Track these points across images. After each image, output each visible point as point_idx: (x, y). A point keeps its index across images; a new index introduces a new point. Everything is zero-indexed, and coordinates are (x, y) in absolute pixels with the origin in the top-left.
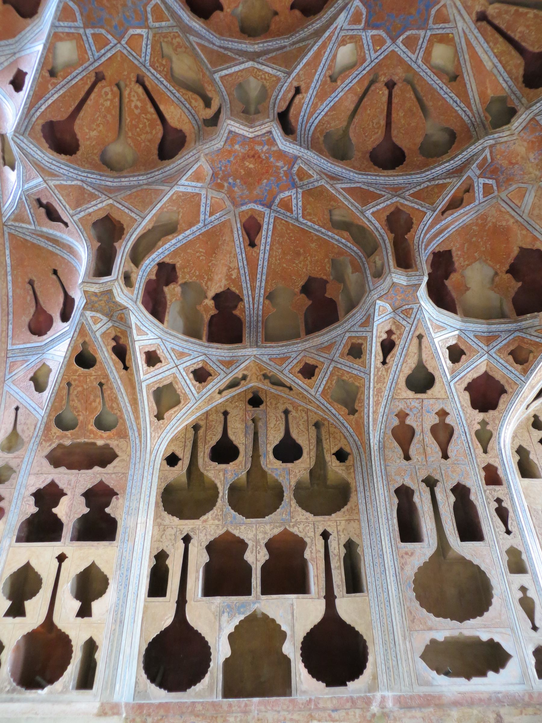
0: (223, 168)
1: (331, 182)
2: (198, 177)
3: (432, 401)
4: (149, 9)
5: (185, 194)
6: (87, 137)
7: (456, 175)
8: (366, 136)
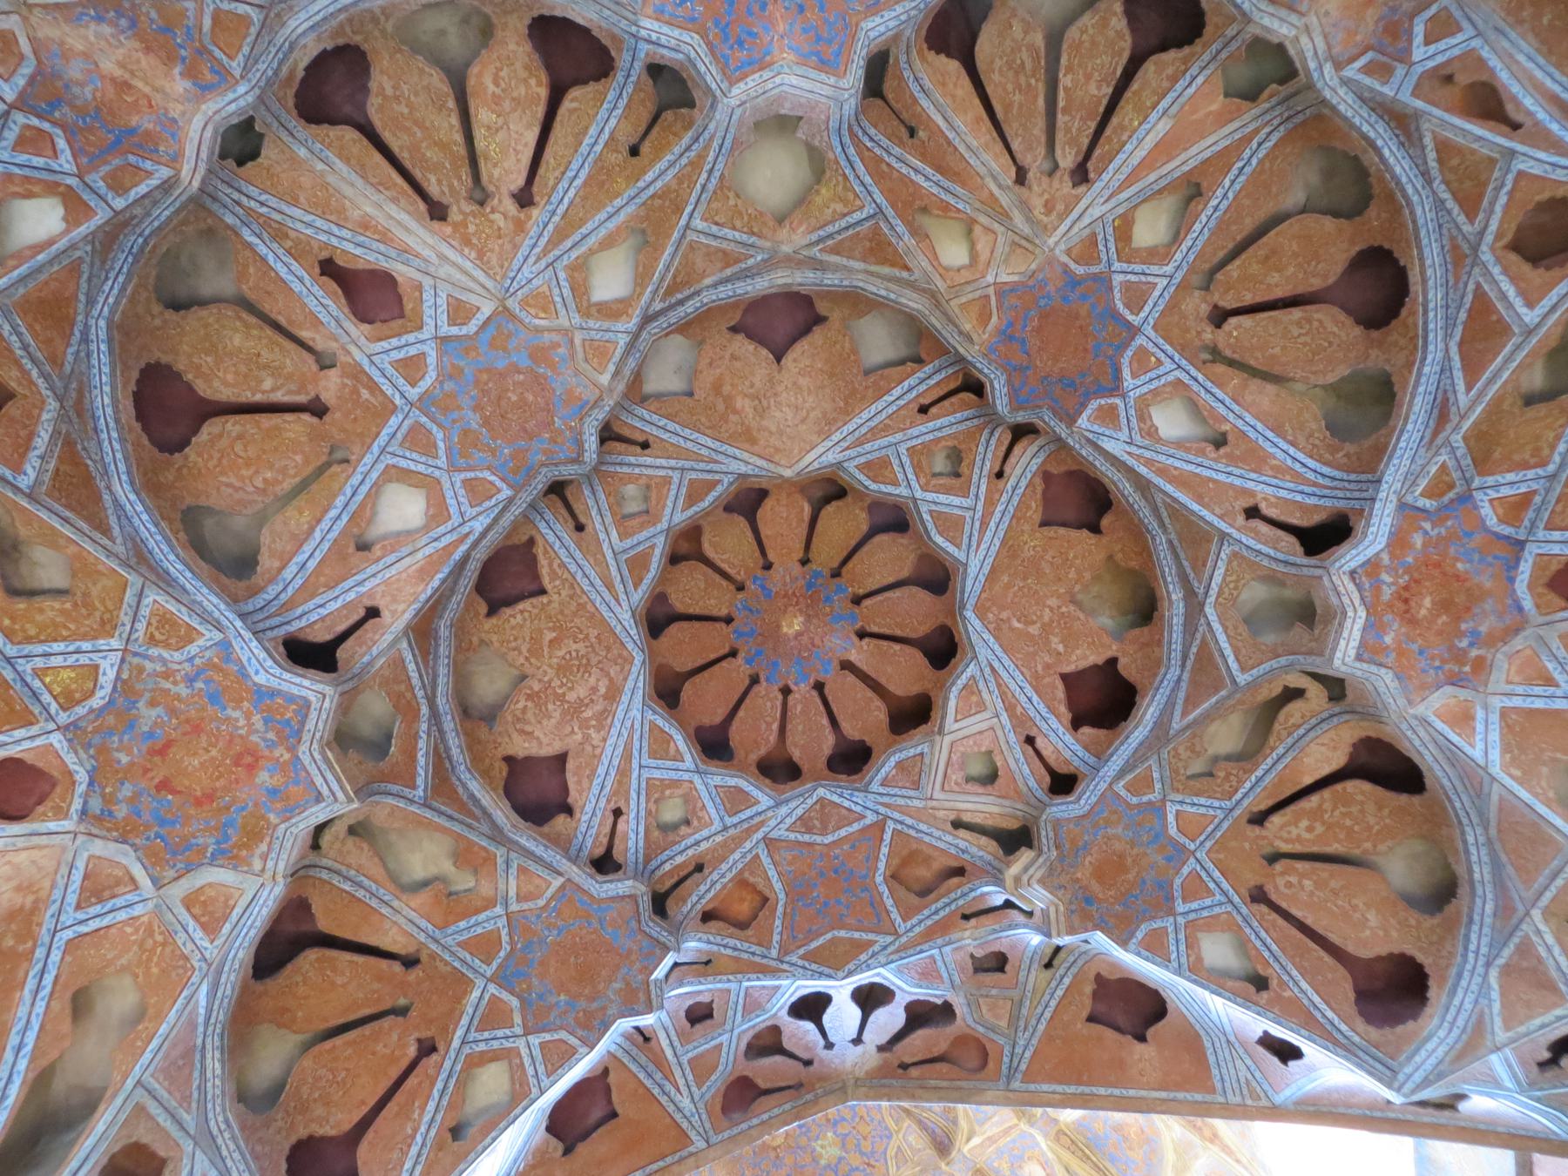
0: (1437, 663)
1: (1455, 419)
2: (1462, 719)
4: (1135, 800)
5: (1506, 749)
6: (1381, 933)
7: (1413, 128)
8: (1330, 344)
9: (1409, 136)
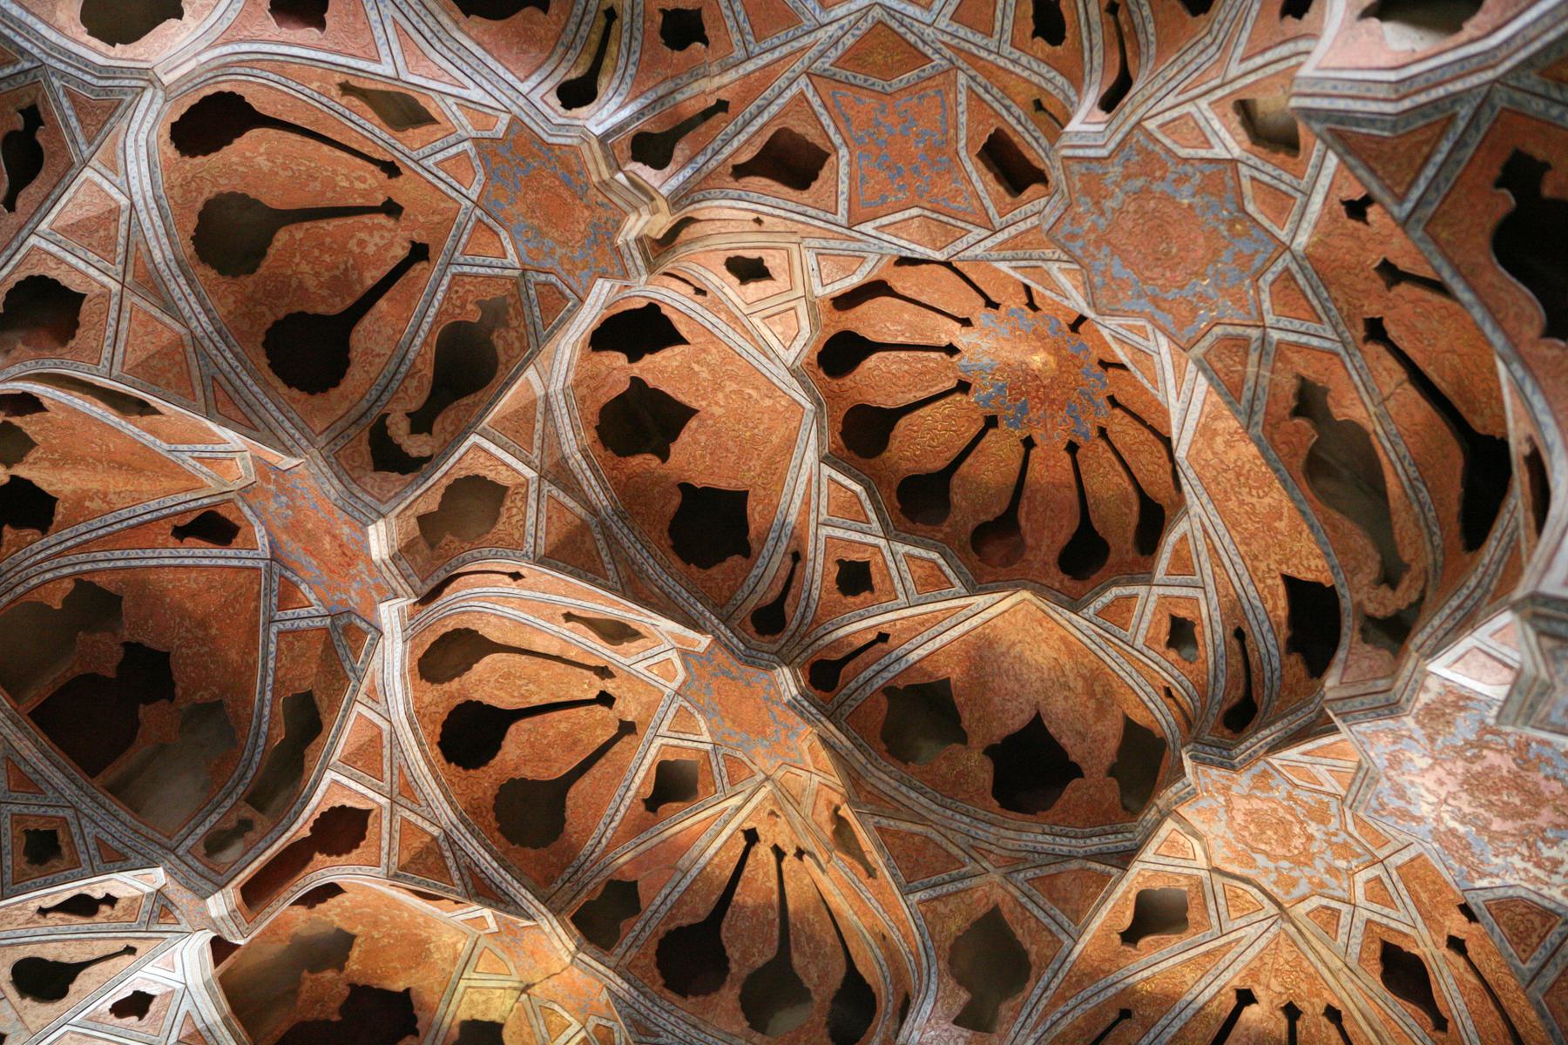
3: (9, 1012)
7: (470, 886)
9: (473, 875)
